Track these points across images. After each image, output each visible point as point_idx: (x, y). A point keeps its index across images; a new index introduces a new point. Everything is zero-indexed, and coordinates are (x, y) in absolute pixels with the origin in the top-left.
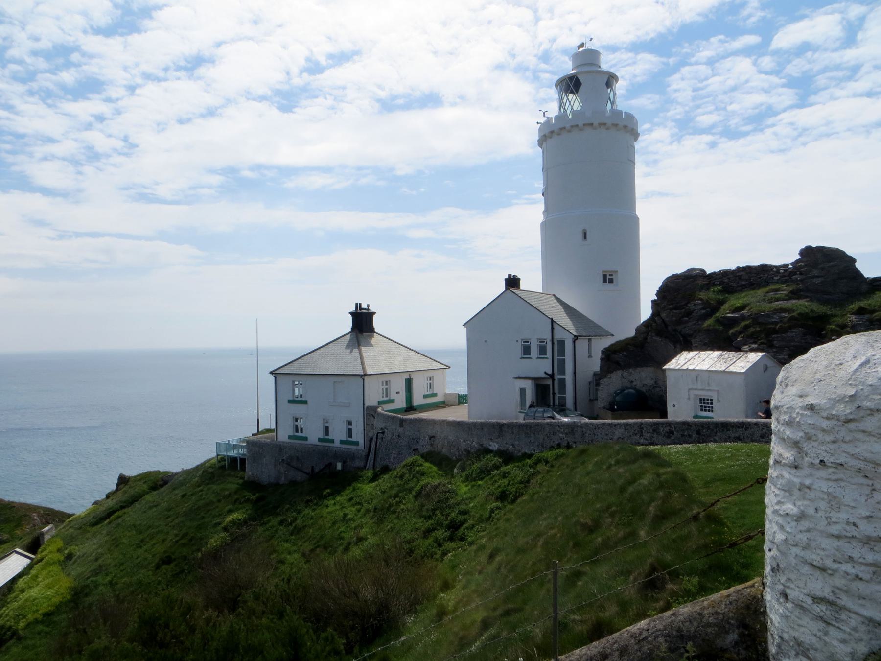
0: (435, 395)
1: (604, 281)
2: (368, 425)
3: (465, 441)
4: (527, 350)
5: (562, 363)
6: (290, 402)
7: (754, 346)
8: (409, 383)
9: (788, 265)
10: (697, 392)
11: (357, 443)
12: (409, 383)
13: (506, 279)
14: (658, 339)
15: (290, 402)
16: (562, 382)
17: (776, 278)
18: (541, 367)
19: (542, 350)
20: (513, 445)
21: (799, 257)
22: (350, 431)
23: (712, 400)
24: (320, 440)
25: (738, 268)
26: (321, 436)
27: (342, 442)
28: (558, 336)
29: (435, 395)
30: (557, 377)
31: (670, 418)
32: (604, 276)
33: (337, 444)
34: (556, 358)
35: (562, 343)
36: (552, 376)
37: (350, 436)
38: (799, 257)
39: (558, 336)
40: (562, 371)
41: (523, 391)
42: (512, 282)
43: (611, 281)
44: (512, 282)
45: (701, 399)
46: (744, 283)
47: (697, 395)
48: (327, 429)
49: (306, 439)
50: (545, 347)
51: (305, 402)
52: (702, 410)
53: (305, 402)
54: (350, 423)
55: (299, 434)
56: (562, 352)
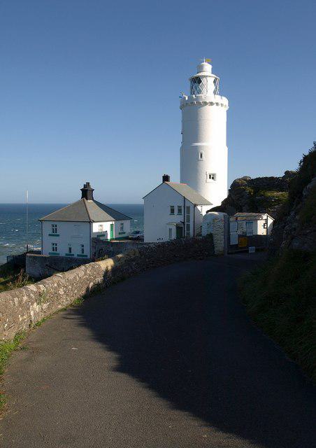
0: (124, 233)
2: (93, 247)
4: (172, 211)
5: (188, 217)
6: (50, 235)
11: (86, 256)
13: (163, 177)
15: (50, 235)
16: (188, 226)
18: (177, 219)
19: (180, 211)
22: (83, 250)
24: (66, 255)
26: (68, 252)
27: (78, 255)
28: (187, 205)
29: (124, 233)
30: (186, 223)
32: (210, 176)
33: (76, 256)
35: (188, 208)
36: (184, 223)
37: (83, 252)
39: (187, 205)
40: (188, 221)
41: (170, 230)
42: (166, 178)
43: (213, 178)
44: (166, 178)
48: (70, 249)
49: (59, 254)
51: (58, 235)
53: (58, 235)
54: (83, 246)
55: (55, 252)
56: (188, 212)
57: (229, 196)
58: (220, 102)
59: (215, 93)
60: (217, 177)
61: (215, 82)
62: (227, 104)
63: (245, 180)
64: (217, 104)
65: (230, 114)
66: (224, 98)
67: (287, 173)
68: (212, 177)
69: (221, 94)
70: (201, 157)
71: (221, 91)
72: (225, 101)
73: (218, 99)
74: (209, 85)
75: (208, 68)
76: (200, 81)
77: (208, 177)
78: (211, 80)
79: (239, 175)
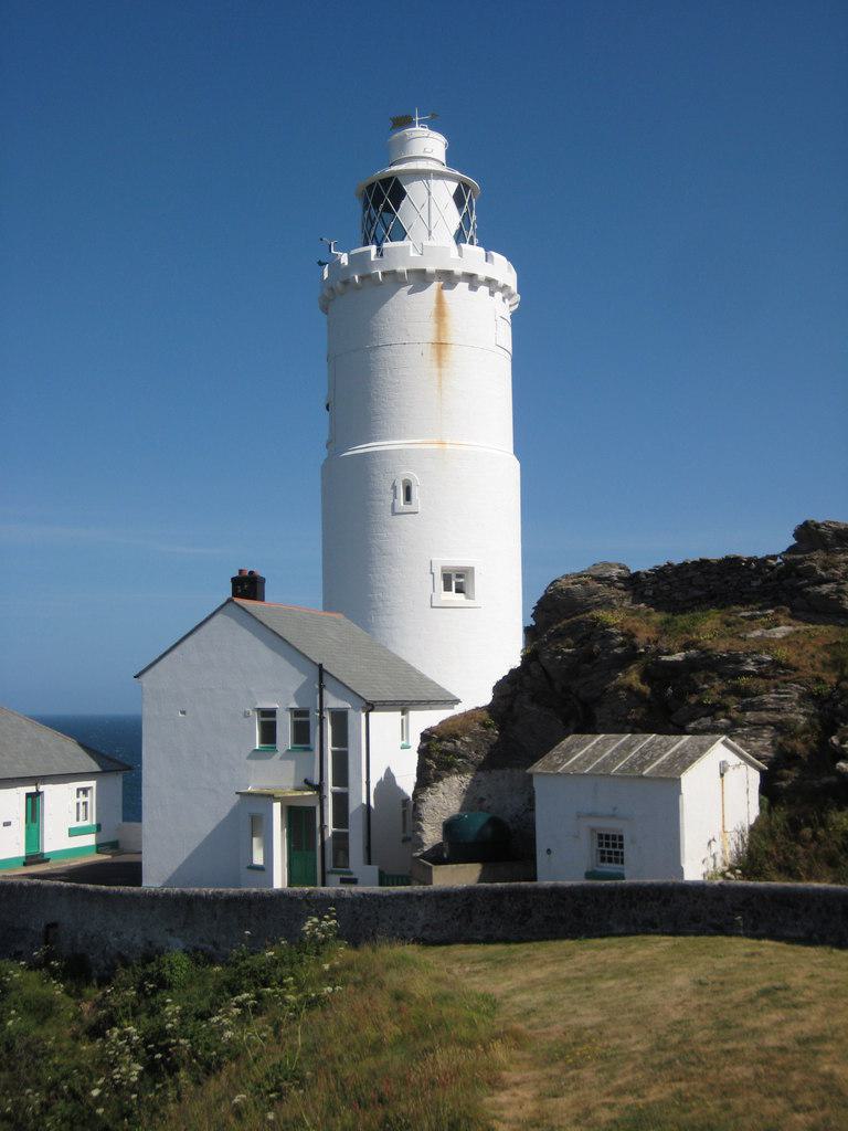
1: (447, 588)
3: (118, 934)
4: (269, 733)
7: (707, 721)
8: (34, 800)
9: (774, 557)
10: (595, 823)
12: (34, 800)
14: (534, 708)
17: (754, 584)
19: (302, 734)
20: (215, 944)
21: (793, 541)
23: (621, 838)
25: (685, 564)
30: (330, 788)
31: (544, 882)
32: (447, 579)
34: (329, 747)
35: (340, 719)
38: (793, 541)
45: (600, 836)
46: (697, 593)
47: (593, 830)
50: (308, 723)
52: (603, 860)
57: (529, 658)
58: (483, 271)
59: (460, 237)
60: (479, 583)
61: (459, 199)
62: (514, 288)
63: (599, 579)
64: (471, 279)
65: (521, 323)
66: (499, 258)
67: (809, 535)
68: (457, 580)
69: (489, 244)
70: (408, 497)
71: (485, 221)
72: (502, 270)
73: (473, 258)
74: (433, 220)
75: (428, 146)
76: (398, 194)
77: (440, 584)
78: (445, 190)
79: (577, 557)
